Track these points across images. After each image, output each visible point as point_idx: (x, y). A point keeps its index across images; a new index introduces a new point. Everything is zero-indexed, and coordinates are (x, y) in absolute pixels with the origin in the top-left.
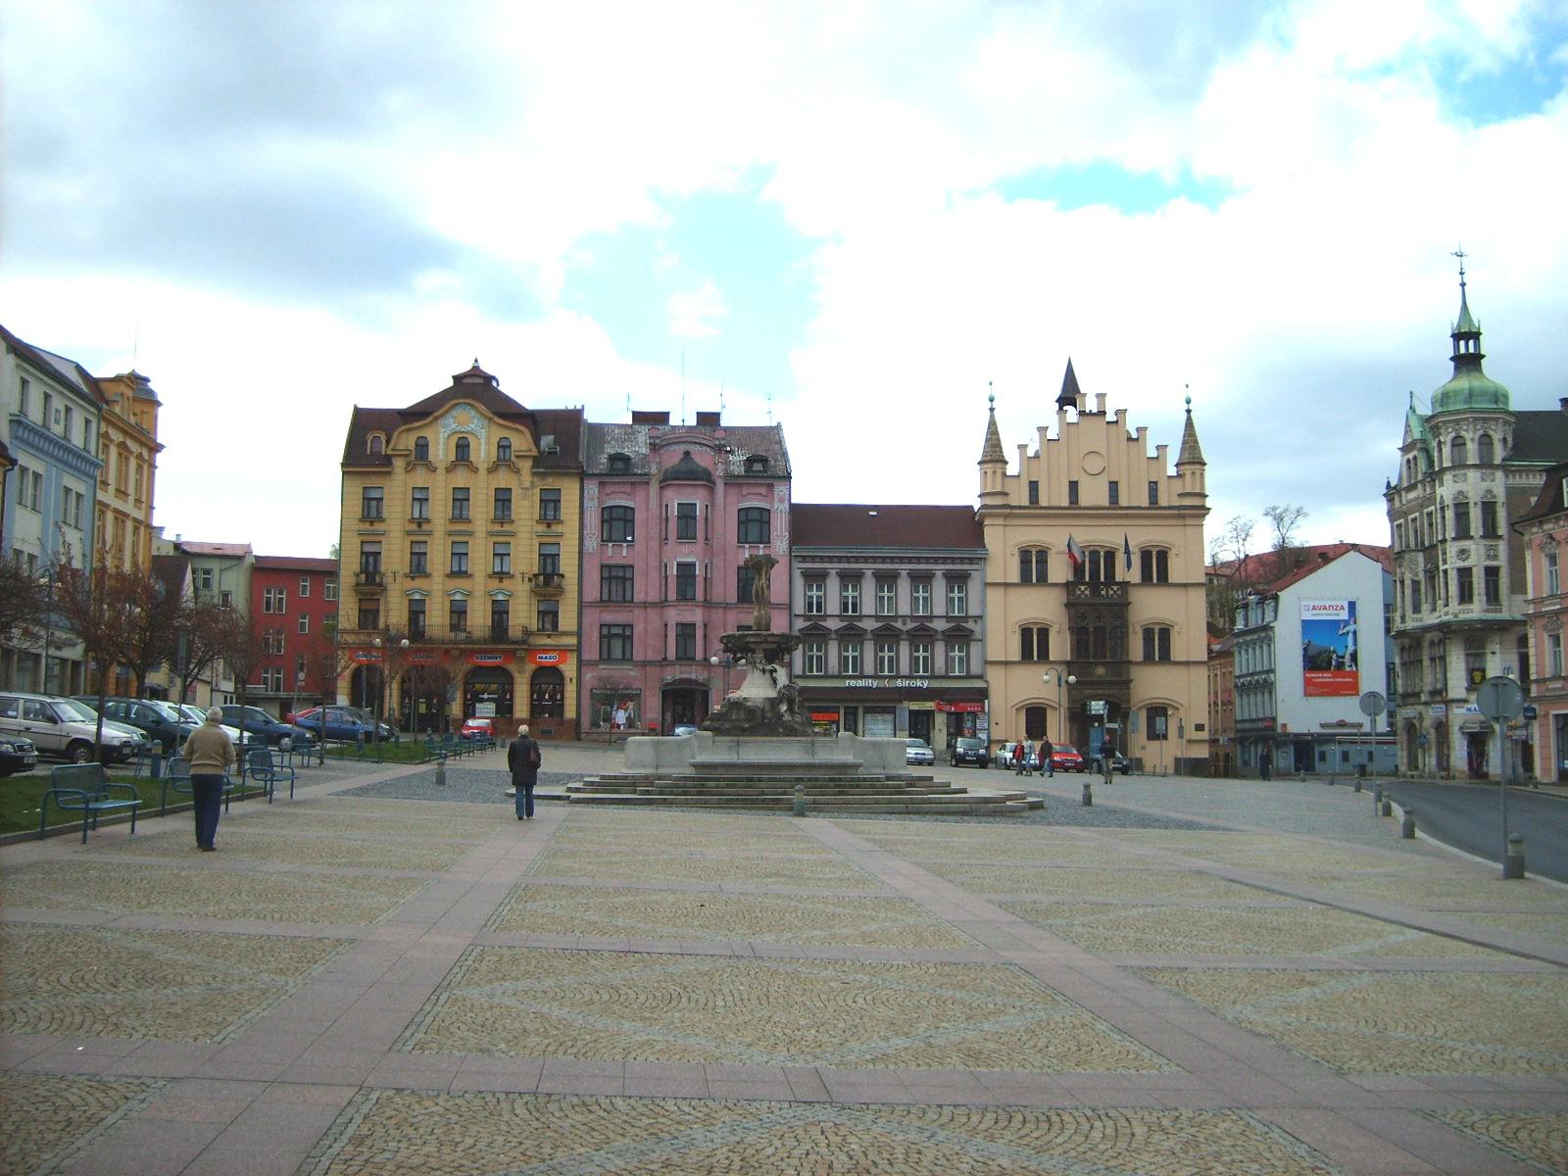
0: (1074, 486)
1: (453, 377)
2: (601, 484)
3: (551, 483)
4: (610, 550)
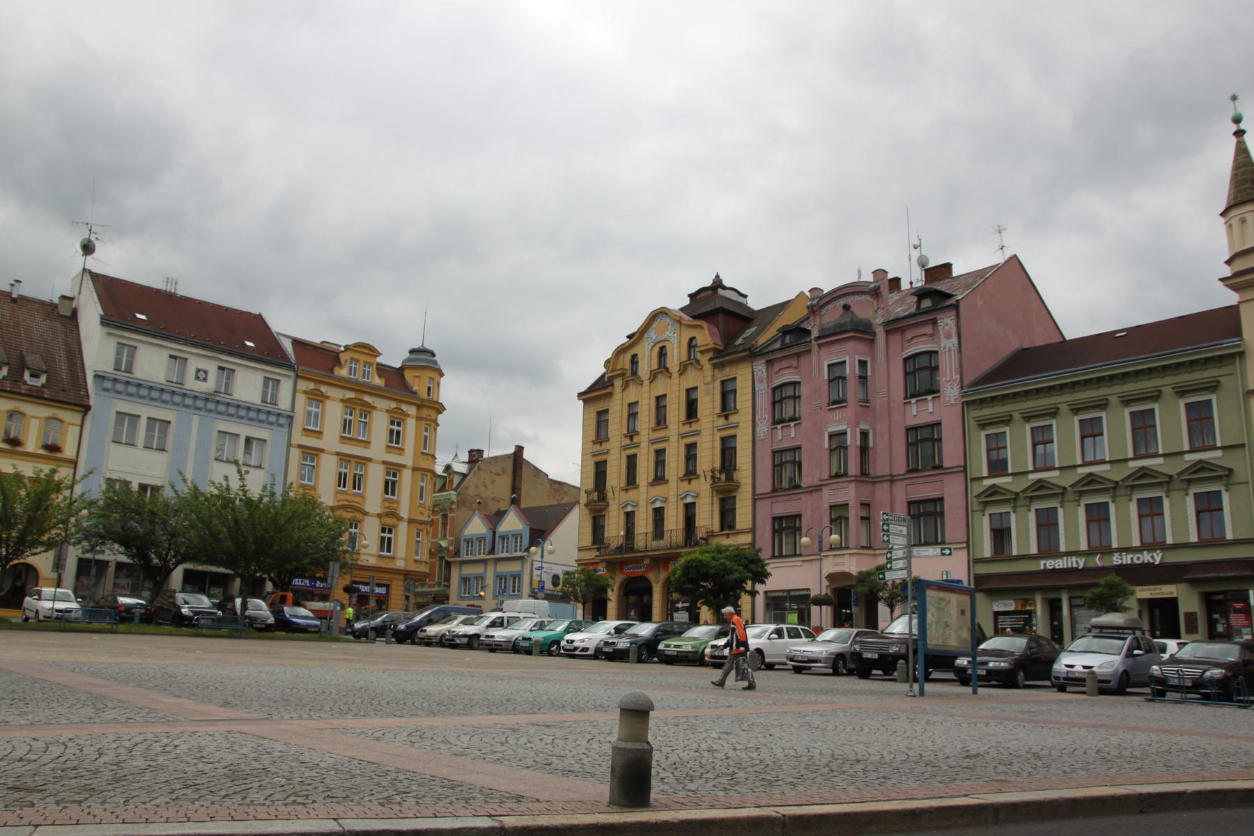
1: (689, 296)
2: (769, 363)
3: (728, 373)
4: (780, 432)
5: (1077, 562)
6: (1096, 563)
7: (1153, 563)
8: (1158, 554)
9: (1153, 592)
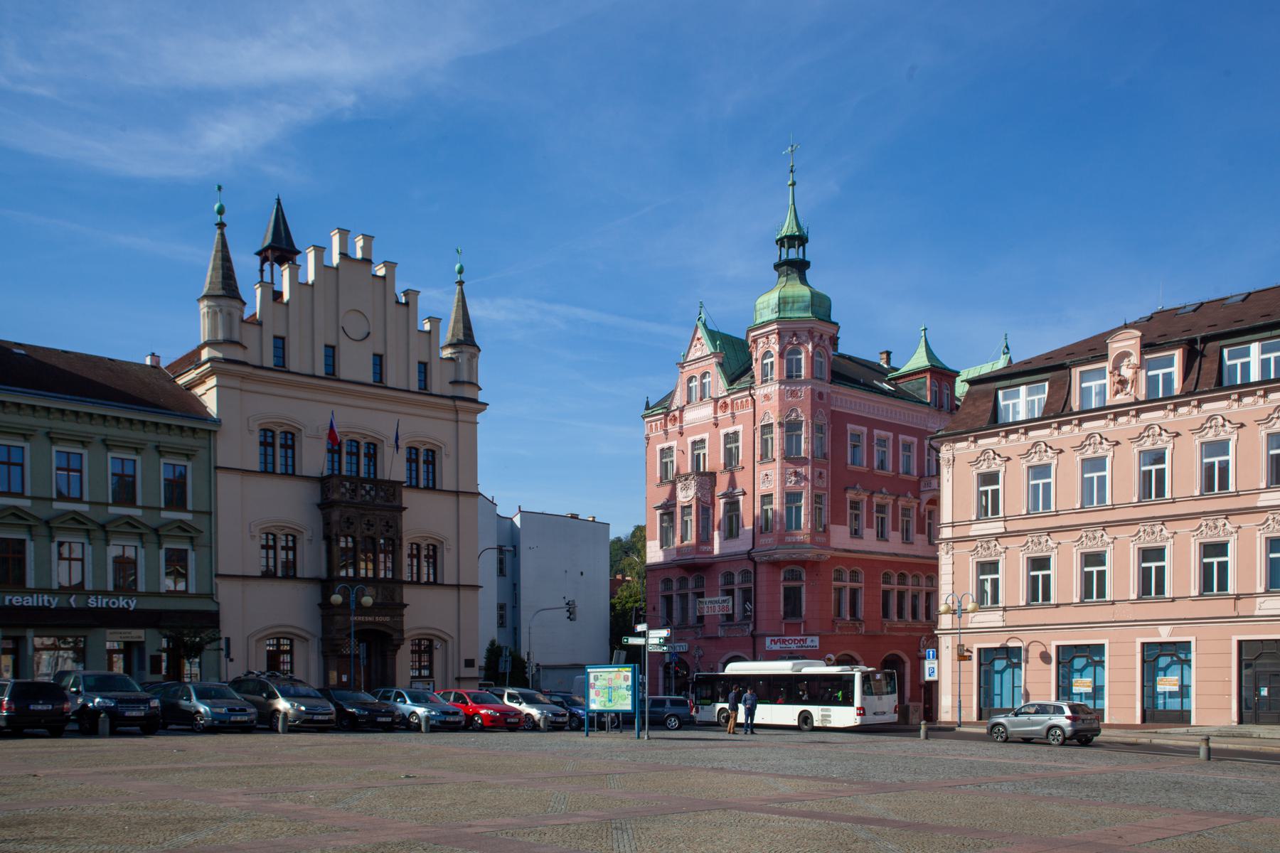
0: (331, 351)
5: (49, 600)
6: (70, 603)
7: (127, 609)
8: (132, 601)
9: (123, 635)
